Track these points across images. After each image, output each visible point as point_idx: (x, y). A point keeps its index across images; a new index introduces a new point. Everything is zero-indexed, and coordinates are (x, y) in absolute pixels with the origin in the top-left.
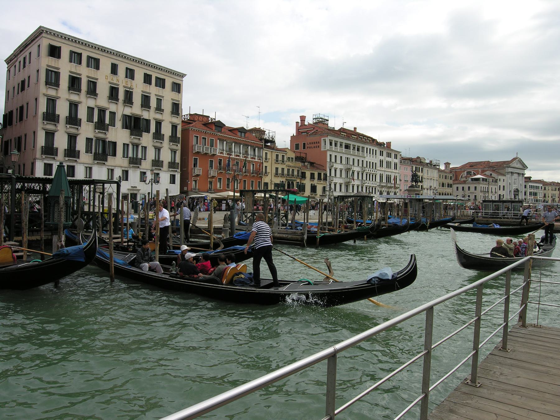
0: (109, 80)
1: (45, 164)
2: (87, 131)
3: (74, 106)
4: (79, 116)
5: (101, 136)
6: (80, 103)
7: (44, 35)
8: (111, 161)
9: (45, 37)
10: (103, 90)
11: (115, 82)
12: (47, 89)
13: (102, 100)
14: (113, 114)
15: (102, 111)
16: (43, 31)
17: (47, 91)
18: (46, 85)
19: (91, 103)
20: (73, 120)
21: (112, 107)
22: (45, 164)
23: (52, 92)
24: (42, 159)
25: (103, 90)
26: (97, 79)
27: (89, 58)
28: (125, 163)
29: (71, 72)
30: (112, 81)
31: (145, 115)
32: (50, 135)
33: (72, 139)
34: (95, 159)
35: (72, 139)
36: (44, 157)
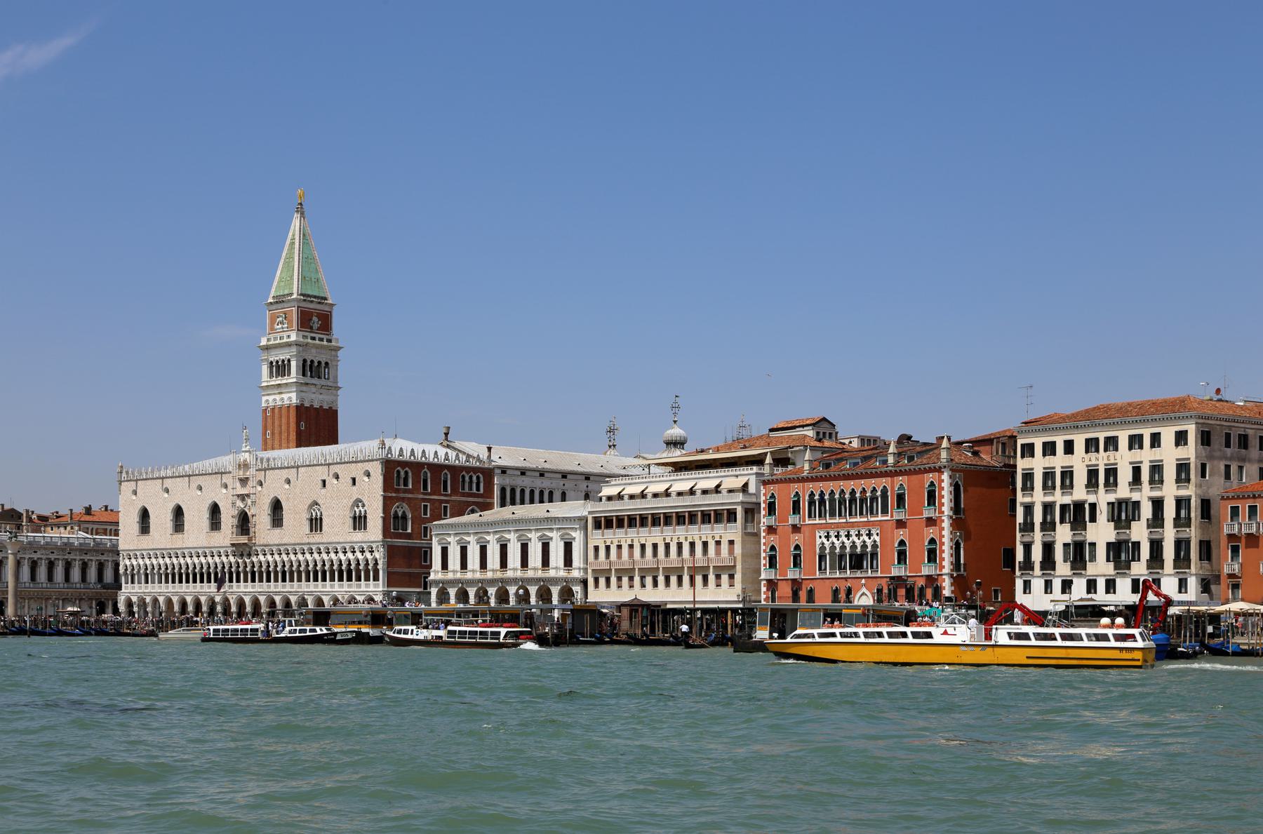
2: (1064, 534)
3: (1048, 508)
8: (1091, 569)
11: (1094, 462)
13: (1079, 492)
14: (1093, 507)
15: (1079, 506)
19: (1067, 500)
20: (1048, 526)
21: (1091, 499)
24: (1020, 577)
28: (1109, 569)
31: (1135, 497)
32: (1028, 547)
33: (1048, 548)
35: (1048, 548)
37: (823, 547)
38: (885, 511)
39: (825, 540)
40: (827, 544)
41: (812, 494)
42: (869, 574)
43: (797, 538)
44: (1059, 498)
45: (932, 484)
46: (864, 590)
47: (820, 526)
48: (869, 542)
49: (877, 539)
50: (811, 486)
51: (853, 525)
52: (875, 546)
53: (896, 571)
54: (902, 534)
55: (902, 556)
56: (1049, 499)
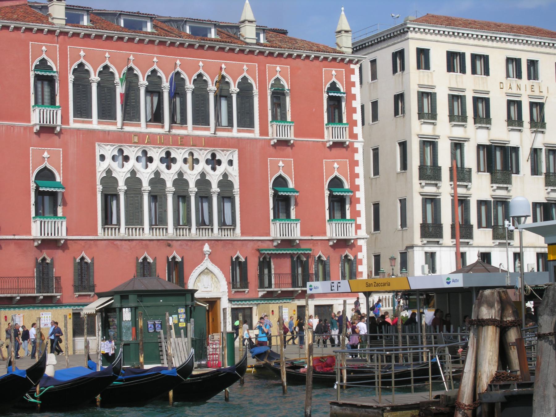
0: (505, 90)
1: (426, 253)
4: (467, 165)
5: (502, 193)
6: (467, 140)
7: (410, 35)
9: (412, 39)
10: (498, 111)
11: (514, 91)
12: (422, 124)
16: (409, 28)
17: (421, 129)
18: (420, 118)
19: (483, 137)
22: (426, 253)
23: (427, 130)
25: (498, 111)
26: (488, 92)
27: (474, 57)
29: (451, 89)
30: (510, 91)
34: (495, 237)
36: (425, 242)
37: (109, 179)
38: (246, 120)
39: (115, 166)
40: (121, 174)
41: (81, 72)
42: (216, 233)
43: (46, 156)
44: (475, 136)
45: (333, 87)
46: (207, 263)
47: (107, 138)
48: (214, 177)
49: (234, 174)
50: (82, 53)
51: (183, 142)
52: (225, 183)
53: (276, 231)
54: (281, 166)
55: (283, 204)
56: (458, 133)
